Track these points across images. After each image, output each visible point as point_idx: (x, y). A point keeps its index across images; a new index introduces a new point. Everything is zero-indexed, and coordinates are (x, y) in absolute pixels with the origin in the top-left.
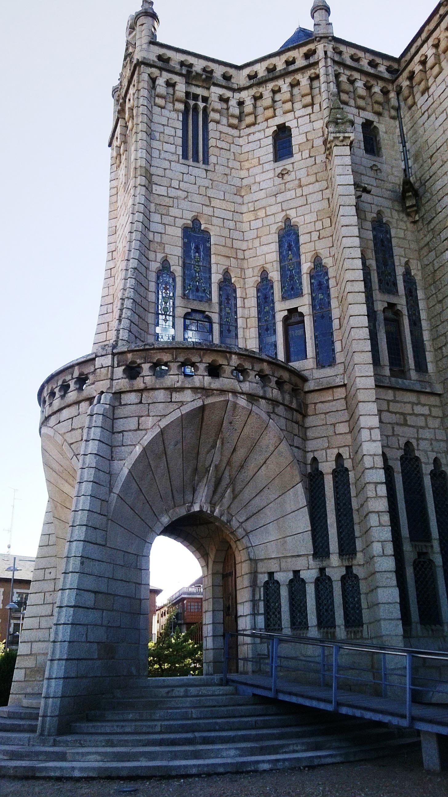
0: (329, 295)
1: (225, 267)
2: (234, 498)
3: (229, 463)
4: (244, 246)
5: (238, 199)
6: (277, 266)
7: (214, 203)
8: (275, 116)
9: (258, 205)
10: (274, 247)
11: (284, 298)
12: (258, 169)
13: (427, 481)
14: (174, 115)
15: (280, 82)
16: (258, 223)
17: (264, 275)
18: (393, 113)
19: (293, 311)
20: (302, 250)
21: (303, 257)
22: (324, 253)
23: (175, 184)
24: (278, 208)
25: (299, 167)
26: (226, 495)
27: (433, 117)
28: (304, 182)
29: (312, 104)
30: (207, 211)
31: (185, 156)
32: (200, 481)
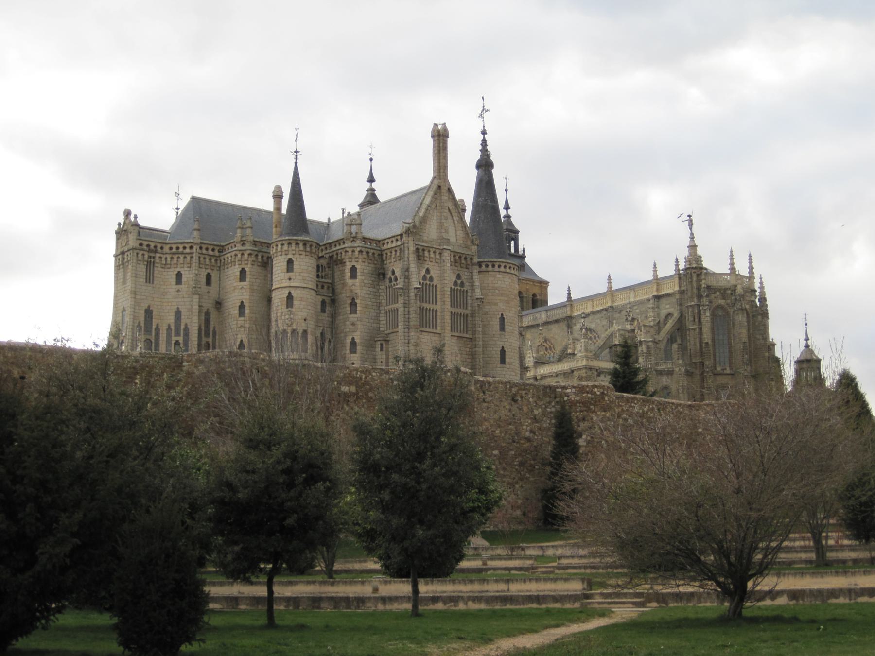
4: (163, 314)
5: (163, 297)
7: (155, 299)
14: (143, 266)
15: (180, 255)
17: (169, 326)
18: (218, 269)
19: (177, 341)
20: (182, 321)
22: (188, 324)
23: (143, 294)
24: (175, 304)
28: (185, 296)
29: (190, 267)
31: (146, 282)
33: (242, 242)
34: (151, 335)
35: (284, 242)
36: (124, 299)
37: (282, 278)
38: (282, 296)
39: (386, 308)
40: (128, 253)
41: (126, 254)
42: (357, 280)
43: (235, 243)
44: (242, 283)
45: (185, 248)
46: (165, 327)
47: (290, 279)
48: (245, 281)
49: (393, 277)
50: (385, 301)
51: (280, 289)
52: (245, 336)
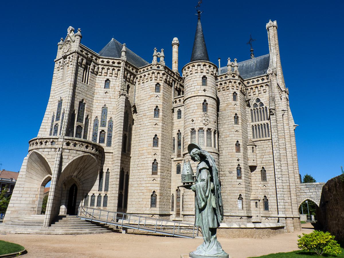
0: (112, 129)
1: (87, 114)
2: (82, 175)
3: (84, 168)
6: (100, 117)
8: (106, 76)
9: (98, 99)
10: (101, 112)
11: (101, 126)
12: (100, 89)
13: (125, 176)
15: (110, 67)
16: (97, 104)
21: (108, 117)
25: (111, 93)
26: (81, 174)
27: (143, 91)
30: (86, 98)
32: (76, 171)
33: (157, 65)
34: (83, 123)
35: (200, 63)
36: (62, 92)
37: (198, 89)
38: (199, 102)
39: (251, 124)
40: (71, 56)
41: (68, 57)
42: (238, 102)
43: (152, 66)
44: (158, 94)
45: (113, 63)
46: (93, 119)
47: (205, 90)
48: (159, 92)
49: (258, 104)
50: (250, 119)
51: (197, 97)
52: (160, 132)
